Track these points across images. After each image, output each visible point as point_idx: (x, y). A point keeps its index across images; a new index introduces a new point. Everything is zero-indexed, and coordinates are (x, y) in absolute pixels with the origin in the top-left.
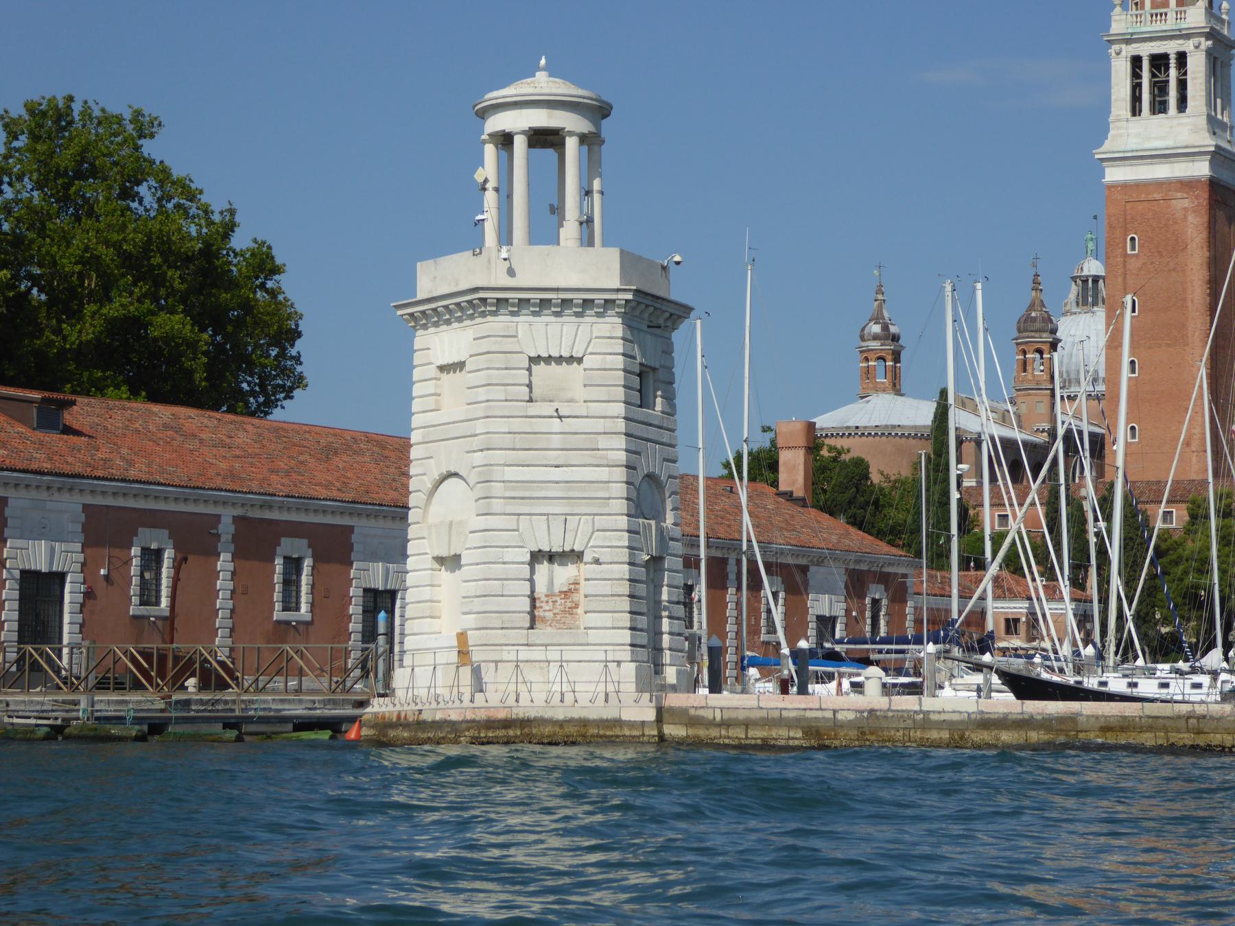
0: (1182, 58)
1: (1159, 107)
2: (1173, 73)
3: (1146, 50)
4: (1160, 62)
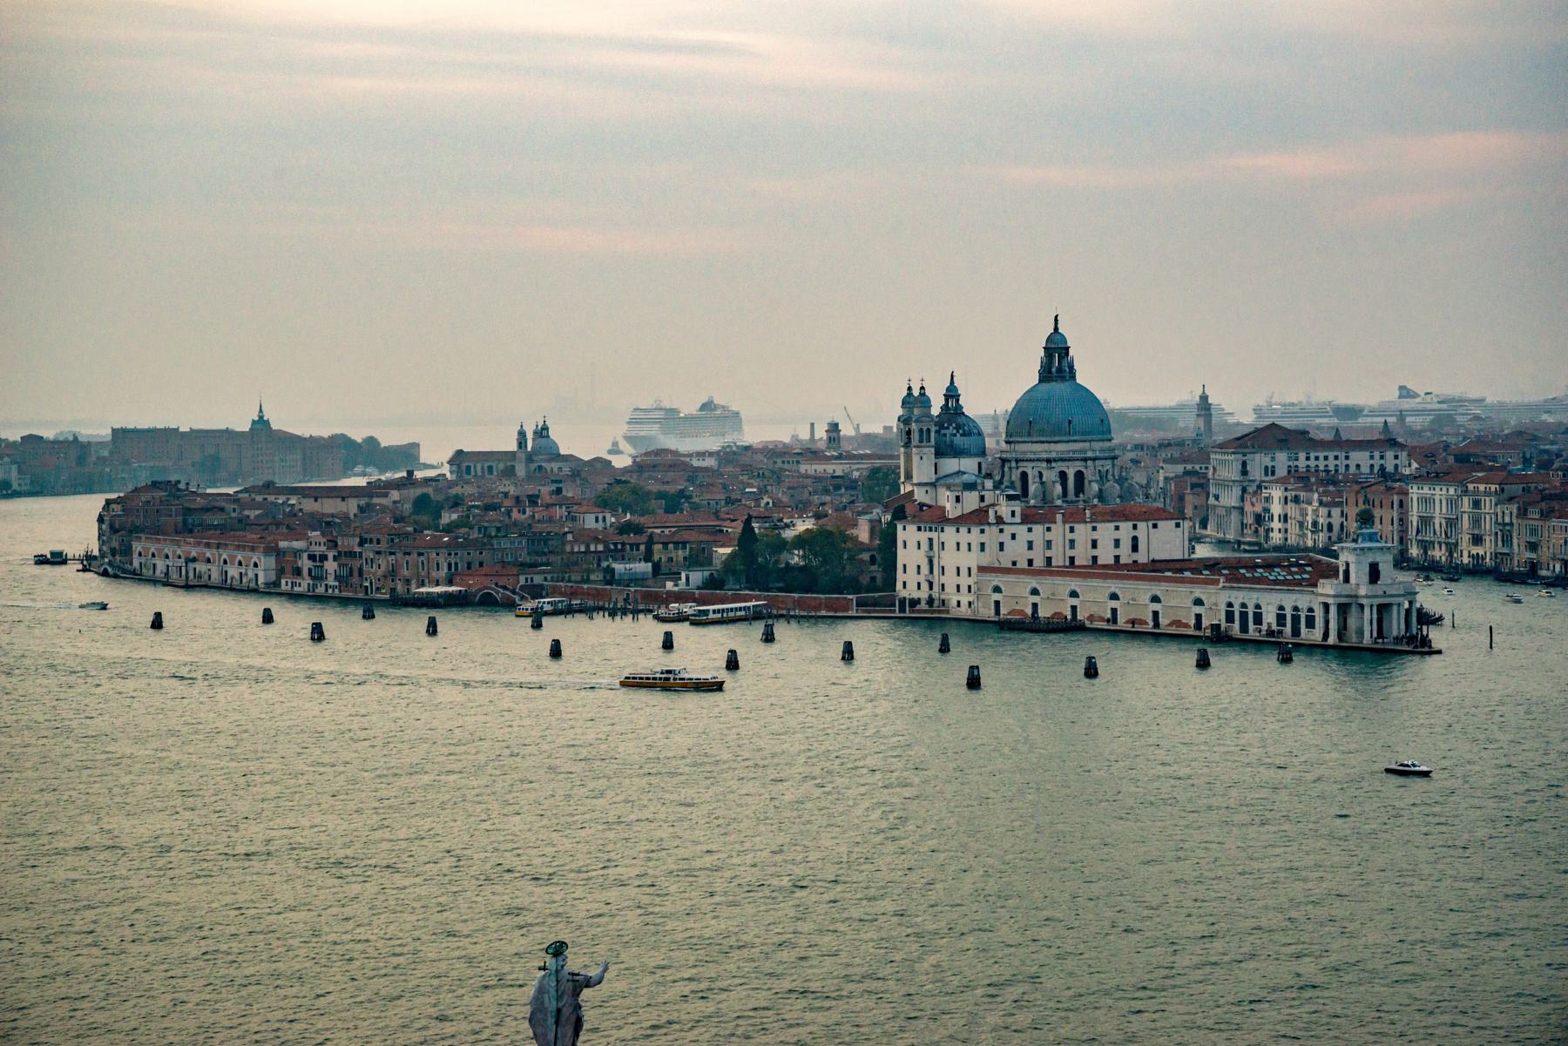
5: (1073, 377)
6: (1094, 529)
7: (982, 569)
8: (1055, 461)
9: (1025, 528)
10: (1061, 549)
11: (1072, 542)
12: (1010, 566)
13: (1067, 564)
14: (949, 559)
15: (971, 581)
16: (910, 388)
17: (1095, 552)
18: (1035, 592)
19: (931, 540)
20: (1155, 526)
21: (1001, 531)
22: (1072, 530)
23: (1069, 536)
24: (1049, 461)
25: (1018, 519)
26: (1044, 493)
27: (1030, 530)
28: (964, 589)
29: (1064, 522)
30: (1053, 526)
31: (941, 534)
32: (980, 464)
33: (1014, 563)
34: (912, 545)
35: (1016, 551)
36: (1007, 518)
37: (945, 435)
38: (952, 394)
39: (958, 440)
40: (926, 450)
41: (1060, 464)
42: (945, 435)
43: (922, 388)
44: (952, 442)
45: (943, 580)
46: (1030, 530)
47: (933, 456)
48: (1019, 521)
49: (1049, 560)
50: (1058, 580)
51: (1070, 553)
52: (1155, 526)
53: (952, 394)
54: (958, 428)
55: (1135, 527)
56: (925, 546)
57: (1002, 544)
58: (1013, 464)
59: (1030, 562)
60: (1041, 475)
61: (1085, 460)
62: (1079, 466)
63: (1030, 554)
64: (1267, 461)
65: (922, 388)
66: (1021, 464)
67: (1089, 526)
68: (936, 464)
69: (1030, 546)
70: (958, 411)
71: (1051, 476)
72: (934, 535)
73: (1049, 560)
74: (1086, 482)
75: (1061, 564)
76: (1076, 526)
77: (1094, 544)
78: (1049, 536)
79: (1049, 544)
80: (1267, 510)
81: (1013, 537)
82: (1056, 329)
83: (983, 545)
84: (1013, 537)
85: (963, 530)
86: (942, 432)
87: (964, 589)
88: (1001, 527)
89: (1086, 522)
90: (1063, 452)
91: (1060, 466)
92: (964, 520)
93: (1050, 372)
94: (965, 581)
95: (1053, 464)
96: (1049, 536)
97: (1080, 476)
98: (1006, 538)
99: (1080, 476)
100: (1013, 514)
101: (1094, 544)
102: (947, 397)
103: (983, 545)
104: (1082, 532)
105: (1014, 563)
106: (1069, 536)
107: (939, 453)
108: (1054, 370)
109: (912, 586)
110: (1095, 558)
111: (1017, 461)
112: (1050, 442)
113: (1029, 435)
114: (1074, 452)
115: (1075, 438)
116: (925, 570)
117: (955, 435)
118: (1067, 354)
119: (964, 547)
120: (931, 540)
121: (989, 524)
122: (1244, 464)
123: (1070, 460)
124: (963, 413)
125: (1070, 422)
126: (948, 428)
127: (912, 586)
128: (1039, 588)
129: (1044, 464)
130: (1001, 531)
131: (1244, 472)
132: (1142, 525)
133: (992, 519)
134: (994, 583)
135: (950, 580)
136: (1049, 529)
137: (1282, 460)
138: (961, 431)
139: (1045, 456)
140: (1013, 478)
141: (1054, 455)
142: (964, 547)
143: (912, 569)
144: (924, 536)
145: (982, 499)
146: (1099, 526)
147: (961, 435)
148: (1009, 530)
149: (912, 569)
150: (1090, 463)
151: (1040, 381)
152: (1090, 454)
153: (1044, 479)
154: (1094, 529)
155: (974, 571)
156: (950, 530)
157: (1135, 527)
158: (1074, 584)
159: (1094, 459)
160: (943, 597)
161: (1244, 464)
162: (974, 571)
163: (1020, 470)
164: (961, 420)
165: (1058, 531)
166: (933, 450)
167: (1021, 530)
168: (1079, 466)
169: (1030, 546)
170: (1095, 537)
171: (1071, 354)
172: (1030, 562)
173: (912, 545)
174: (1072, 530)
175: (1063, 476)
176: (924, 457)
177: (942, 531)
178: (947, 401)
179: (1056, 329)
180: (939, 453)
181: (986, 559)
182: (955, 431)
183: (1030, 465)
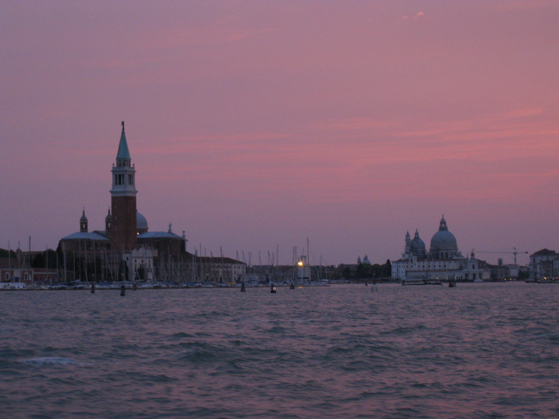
0: (123, 175)
1: (120, 183)
2: (122, 177)
3: (118, 174)
4: (120, 176)
19: (398, 266)
20: (450, 262)
23: (428, 264)
30: (425, 262)
38: (417, 234)
51: (428, 268)
52: (450, 262)
53: (417, 234)
55: (445, 263)
56: (397, 267)
64: (541, 259)
69: (419, 266)
80: (536, 271)
84: (415, 264)
97: (447, 254)
104: (431, 263)
106: (428, 264)
120: (398, 266)
122: (534, 259)
131: (534, 262)
132: (447, 262)
133: (410, 260)
137: (545, 258)
149: (394, 273)
154: (434, 263)
157: (445, 263)
161: (534, 259)
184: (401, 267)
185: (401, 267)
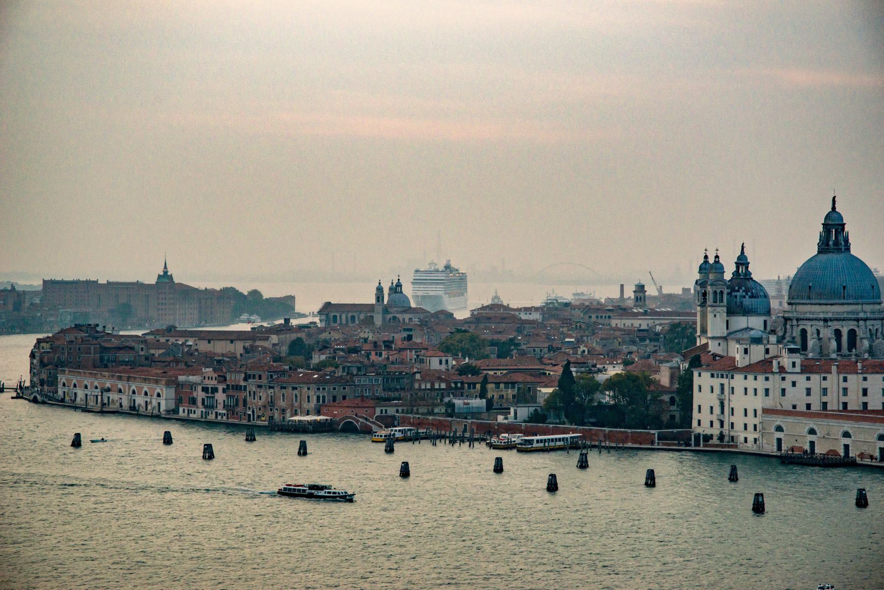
5: (848, 249)
6: (865, 379)
7: (766, 411)
8: (831, 320)
9: (804, 376)
10: (835, 395)
11: (845, 390)
12: (791, 408)
13: (841, 408)
14: (738, 401)
15: (757, 421)
16: (706, 257)
17: (865, 399)
18: (812, 432)
19: (722, 385)
21: (783, 379)
22: (845, 380)
23: (843, 385)
24: (825, 320)
25: (798, 369)
26: (821, 346)
27: (808, 379)
28: (750, 428)
29: (839, 373)
30: (829, 376)
31: (731, 380)
32: (765, 322)
33: (794, 407)
34: (706, 389)
35: (796, 396)
36: (789, 368)
37: (736, 297)
38: (742, 262)
39: (747, 301)
40: (719, 309)
41: (835, 323)
42: (736, 297)
43: (717, 257)
44: (741, 303)
45: (733, 419)
46: (808, 379)
47: (725, 314)
48: (799, 371)
49: (825, 405)
50: (833, 422)
51: (843, 399)
53: (742, 262)
54: (746, 291)
56: (717, 390)
57: (783, 390)
58: (795, 322)
59: (808, 406)
60: (818, 332)
61: (858, 320)
62: (852, 325)
63: (809, 400)
65: (717, 257)
66: (801, 322)
67: (861, 377)
68: (727, 321)
70: (748, 276)
71: (827, 333)
72: (725, 381)
73: (825, 405)
74: (858, 338)
75: (835, 408)
76: (849, 377)
77: (865, 392)
78: (825, 384)
79: (825, 391)
81: (794, 384)
82: (834, 208)
83: (767, 391)
84: (794, 384)
85: (751, 377)
86: (733, 294)
87: (750, 428)
88: (783, 375)
89: (857, 373)
90: (838, 313)
91: (836, 325)
92: (750, 369)
93: (828, 245)
94: (751, 421)
95: (830, 323)
96: (825, 384)
97: (852, 334)
98: (787, 385)
99: (852, 334)
100: (794, 364)
101: (865, 392)
102: (738, 265)
103: (767, 391)
104: (854, 382)
105: (794, 407)
106: (843, 385)
107: (730, 312)
108: (831, 243)
109: (706, 423)
110: (865, 404)
111: (798, 320)
112: (826, 304)
113: (809, 298)
114: (848, 313)
115: (849, 301)
116: (717, 410)
117: (744, 297)
118: (843, 229)
119: (751, 392)
120: (722, 385)
121: (772, 373)
123: (844, 320)
124: (752, 279)
125: (844, 287)
126: (738, 291)
127: (706, 423)
128: (816, 428)
129: (822, 323)
130: (783, 379)
133: (775, 368)
134: (778, 423)
135: (739, 420)
136: (825, 379)
138: (749, 294)
139: (822, 316)
140: (794, 335)
141: (830, 315)
142: (751, 392)
143: (706, 410)
144: (716, 382)
145: (767, 351)
146: (869, 376)
147: (750, 297)
148: (790, 378)
149: (706, 410)
150: (861, 323)
151: (819, 252)
152: (862, 315)
153: (821, 336)
154: (865, 379)
155: (759, 412)
156: (738, 379)
158: (847, 426)
159: (865, 320)
160: (732, 434)
162: (759, 412)
163: (801, 327)
164: (750, 284)
165: (833, 381)
166: (725, 309)
167: (801, 379)
168: (852, 325)
169: (809, 392)
170: (865, 387)
171: (846, 230)
172: (808, 406)
173: (706, 389)
174: (845, 380)
175: (838, 333)
176: (718, 315)
177: (732, 377)
178: (738, 268)
179: (834, 208)
180: (730, 312)
181: (769, 403)
182: (744, 294)
183: (809, 323)
184: (739, 391)
185: (739, 391)
